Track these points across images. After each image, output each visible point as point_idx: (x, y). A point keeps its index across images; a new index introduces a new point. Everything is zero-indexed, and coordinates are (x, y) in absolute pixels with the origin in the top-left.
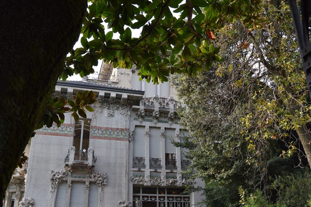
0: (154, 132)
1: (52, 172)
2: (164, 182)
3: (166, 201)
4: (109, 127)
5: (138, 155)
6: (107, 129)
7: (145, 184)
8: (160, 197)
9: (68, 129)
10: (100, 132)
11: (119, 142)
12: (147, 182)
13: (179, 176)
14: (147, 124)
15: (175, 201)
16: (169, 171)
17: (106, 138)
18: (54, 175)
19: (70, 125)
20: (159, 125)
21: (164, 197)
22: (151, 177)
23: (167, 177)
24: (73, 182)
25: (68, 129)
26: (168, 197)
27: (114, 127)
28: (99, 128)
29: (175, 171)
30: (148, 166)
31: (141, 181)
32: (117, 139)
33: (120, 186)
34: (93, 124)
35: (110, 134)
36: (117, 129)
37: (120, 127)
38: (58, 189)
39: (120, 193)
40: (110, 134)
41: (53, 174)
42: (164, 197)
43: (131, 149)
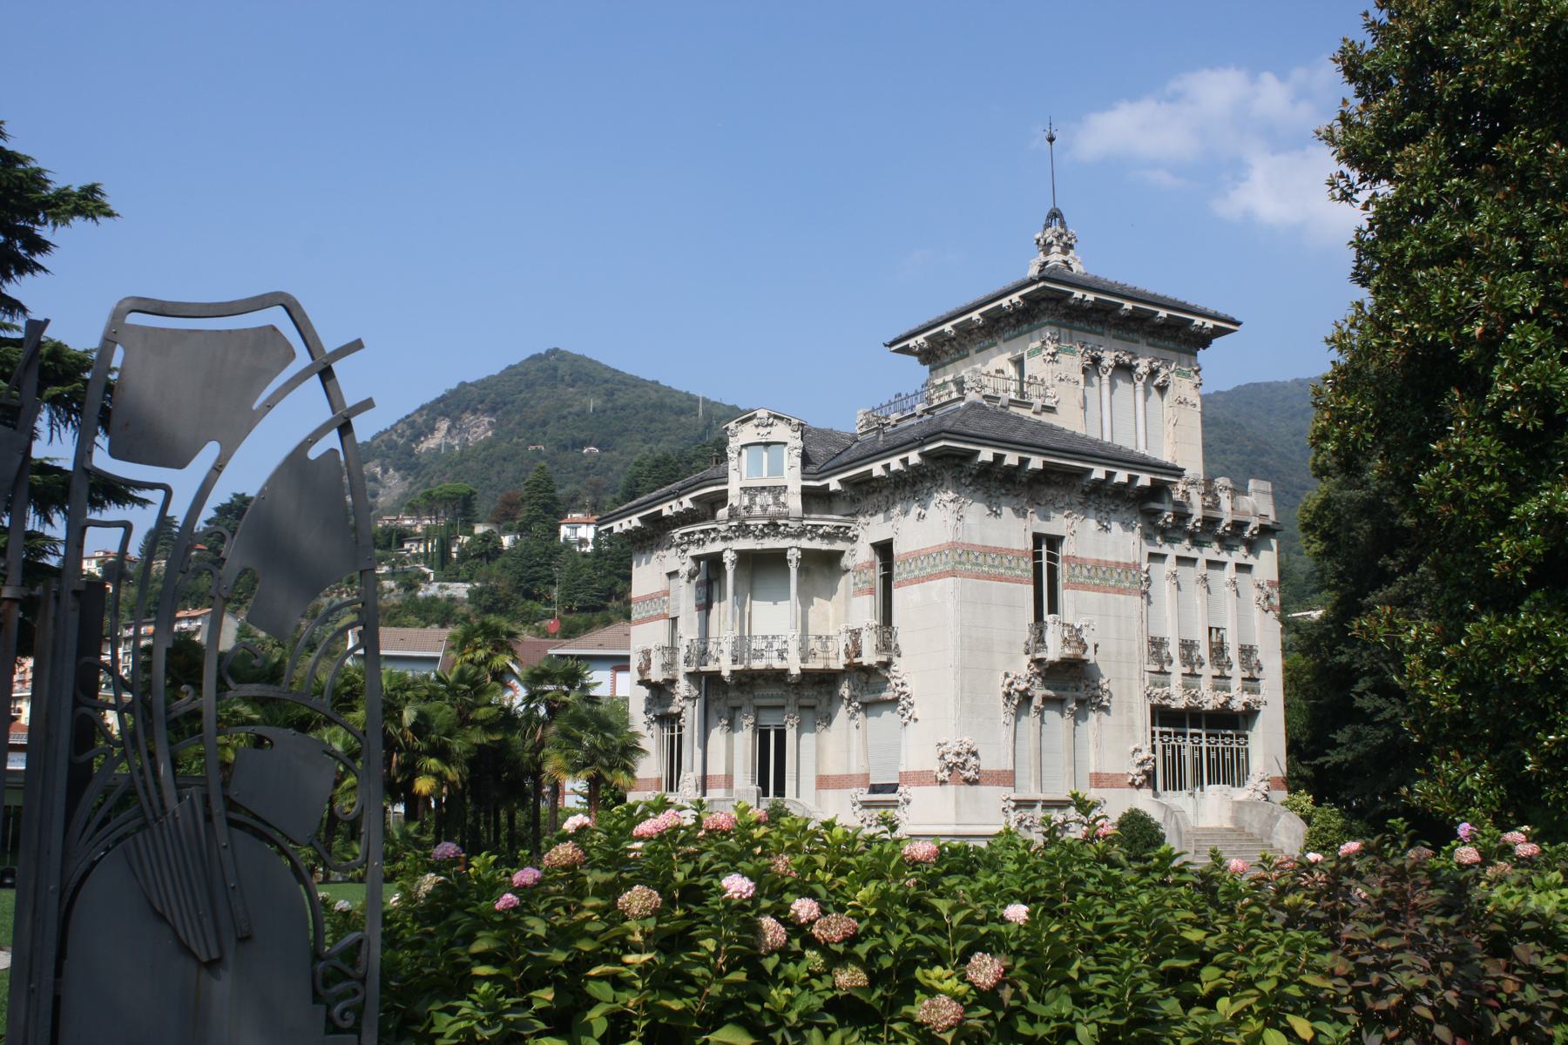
0: (1186, 572)
1: (1007, 675)
2: (1210, 700)
3: (1204, 745)
4: (1102, 558)
5: (1157, 633)
6: (1097, 565)
7: (1174, 705)
8: (1192, 735)
9: (1022, 564)
10: (1085, 572)
11: (1122, 597)
12: (1180, 702)
13: (1236, 684)
14: (1173, 551)
15: (1220, 745)
16: (1217, 673)
17: (1097, 588)
18: (1011, 684)
19: (1024, 553)
20: (1194, 553)
21: (1200, 736)
22: (1186, 686)
23: (1215, 689)
24: (1046, 700)
25: (1022, 564)
26: (1208, 736)
27: (1111, 558)
28: (1082, 563)
29: (1227, 673)
30: (1177, 661)
31: (1168, 697)
32: (1120, 591)
33: (1130, 709)
34: (1065, 550)
35: (1104, 576)
36: (1118, 564)
37: (1122, 560)
38: (1017, 719)
39: (1131, 726)
40: (1104, 576)
41: (1008, 681)
42: (1200, 736)
43: (1145, 619)
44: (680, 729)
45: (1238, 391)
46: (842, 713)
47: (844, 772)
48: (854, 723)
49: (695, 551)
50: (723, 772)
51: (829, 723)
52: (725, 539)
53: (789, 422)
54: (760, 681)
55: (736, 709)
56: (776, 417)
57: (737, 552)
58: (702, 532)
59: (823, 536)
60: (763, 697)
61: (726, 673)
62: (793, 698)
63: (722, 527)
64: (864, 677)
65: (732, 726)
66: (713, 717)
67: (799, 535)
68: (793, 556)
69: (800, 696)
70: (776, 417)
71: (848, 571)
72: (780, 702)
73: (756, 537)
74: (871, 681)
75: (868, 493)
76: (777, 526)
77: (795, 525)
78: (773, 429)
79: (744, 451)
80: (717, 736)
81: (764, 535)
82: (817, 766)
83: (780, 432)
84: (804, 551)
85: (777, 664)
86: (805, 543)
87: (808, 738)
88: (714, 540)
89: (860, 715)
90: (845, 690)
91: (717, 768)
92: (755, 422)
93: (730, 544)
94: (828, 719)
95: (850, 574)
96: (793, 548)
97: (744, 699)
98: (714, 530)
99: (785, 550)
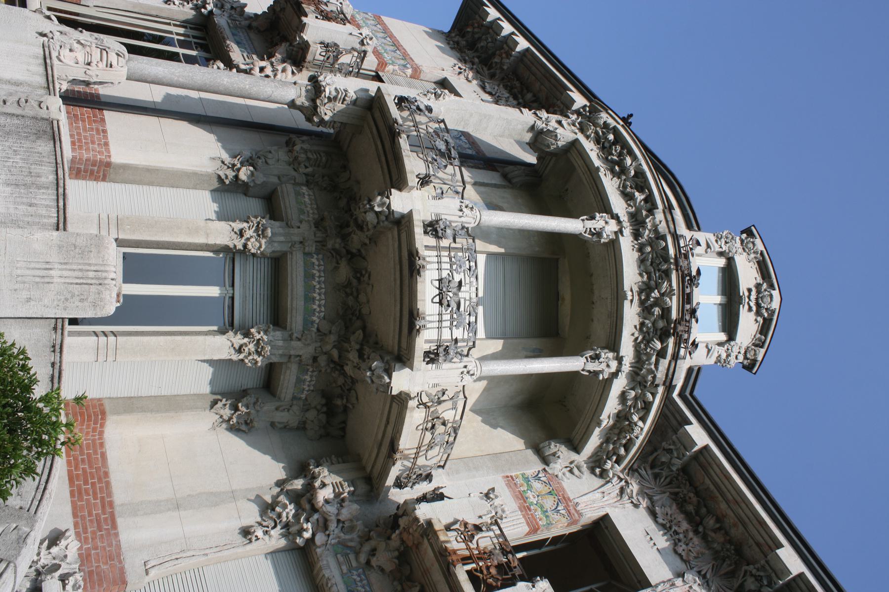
44: (190, 60)
45: (265, 454)
46: (263, 470)
47: (119, 496)
48: (251, 515)
49: (591, 149)
50: (119, 155)
51: (234, 429)
52: (637, 222)
53: (759, 344)
54: (344, 272)
55: (272, 206)
56: (767, 323)
57: (614, 244)
58: (640, 174)
59: (622, 417)
60: (309, 276)
61: (399, 202)
62: (306, 351)
63: (659, 216)
64: (384, 559)
65: (228, 189)
66: (248, 143)
67: (638, 378)
68: (606, 364)
69: (302, 368)
70: (767, 323)
71: (545, 461)
72: (296, 321)
73: (646, 289)
74: (374, 577)
75: (680, 502)
76: (663, 336)
77: (661, 375)
78: (752, 316)
79: (722, 262)
80: (203, 151)
81: (646, 309)
82: (132, 405)
83: (748, 325)
84: (608, 383)
85: (423, 342)
86: (619, 385)
87: (201, 381)
88: (628, 197)
89: (276, 540)
90: (329, 485)
91: (128, 140)
92: (765, 286)
93: (627, 231)
94: (241, 428)
95: (534, 465)
96: (615, 367)
97: (305, 230)
98: (649, 199)
99: (614, 345)
